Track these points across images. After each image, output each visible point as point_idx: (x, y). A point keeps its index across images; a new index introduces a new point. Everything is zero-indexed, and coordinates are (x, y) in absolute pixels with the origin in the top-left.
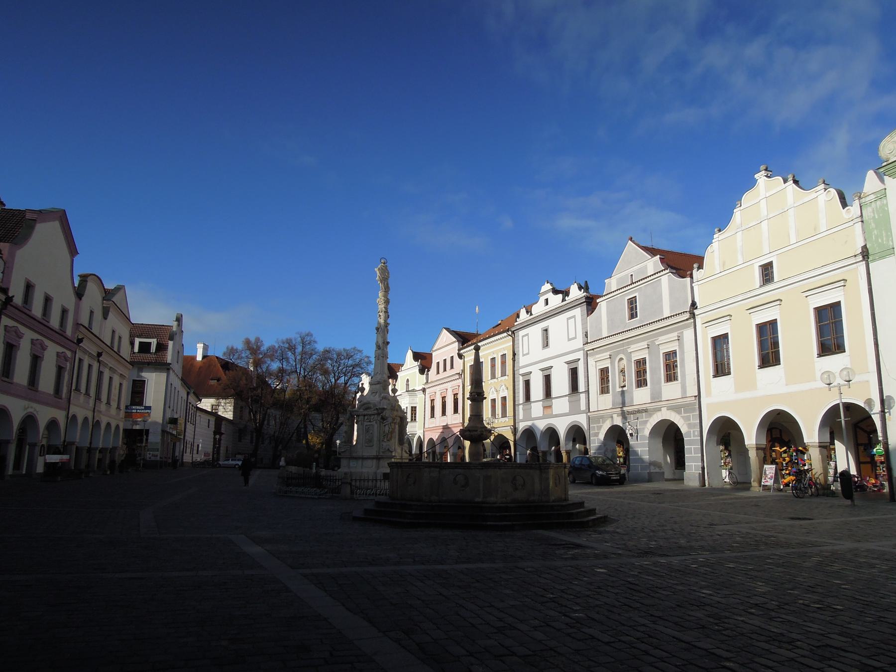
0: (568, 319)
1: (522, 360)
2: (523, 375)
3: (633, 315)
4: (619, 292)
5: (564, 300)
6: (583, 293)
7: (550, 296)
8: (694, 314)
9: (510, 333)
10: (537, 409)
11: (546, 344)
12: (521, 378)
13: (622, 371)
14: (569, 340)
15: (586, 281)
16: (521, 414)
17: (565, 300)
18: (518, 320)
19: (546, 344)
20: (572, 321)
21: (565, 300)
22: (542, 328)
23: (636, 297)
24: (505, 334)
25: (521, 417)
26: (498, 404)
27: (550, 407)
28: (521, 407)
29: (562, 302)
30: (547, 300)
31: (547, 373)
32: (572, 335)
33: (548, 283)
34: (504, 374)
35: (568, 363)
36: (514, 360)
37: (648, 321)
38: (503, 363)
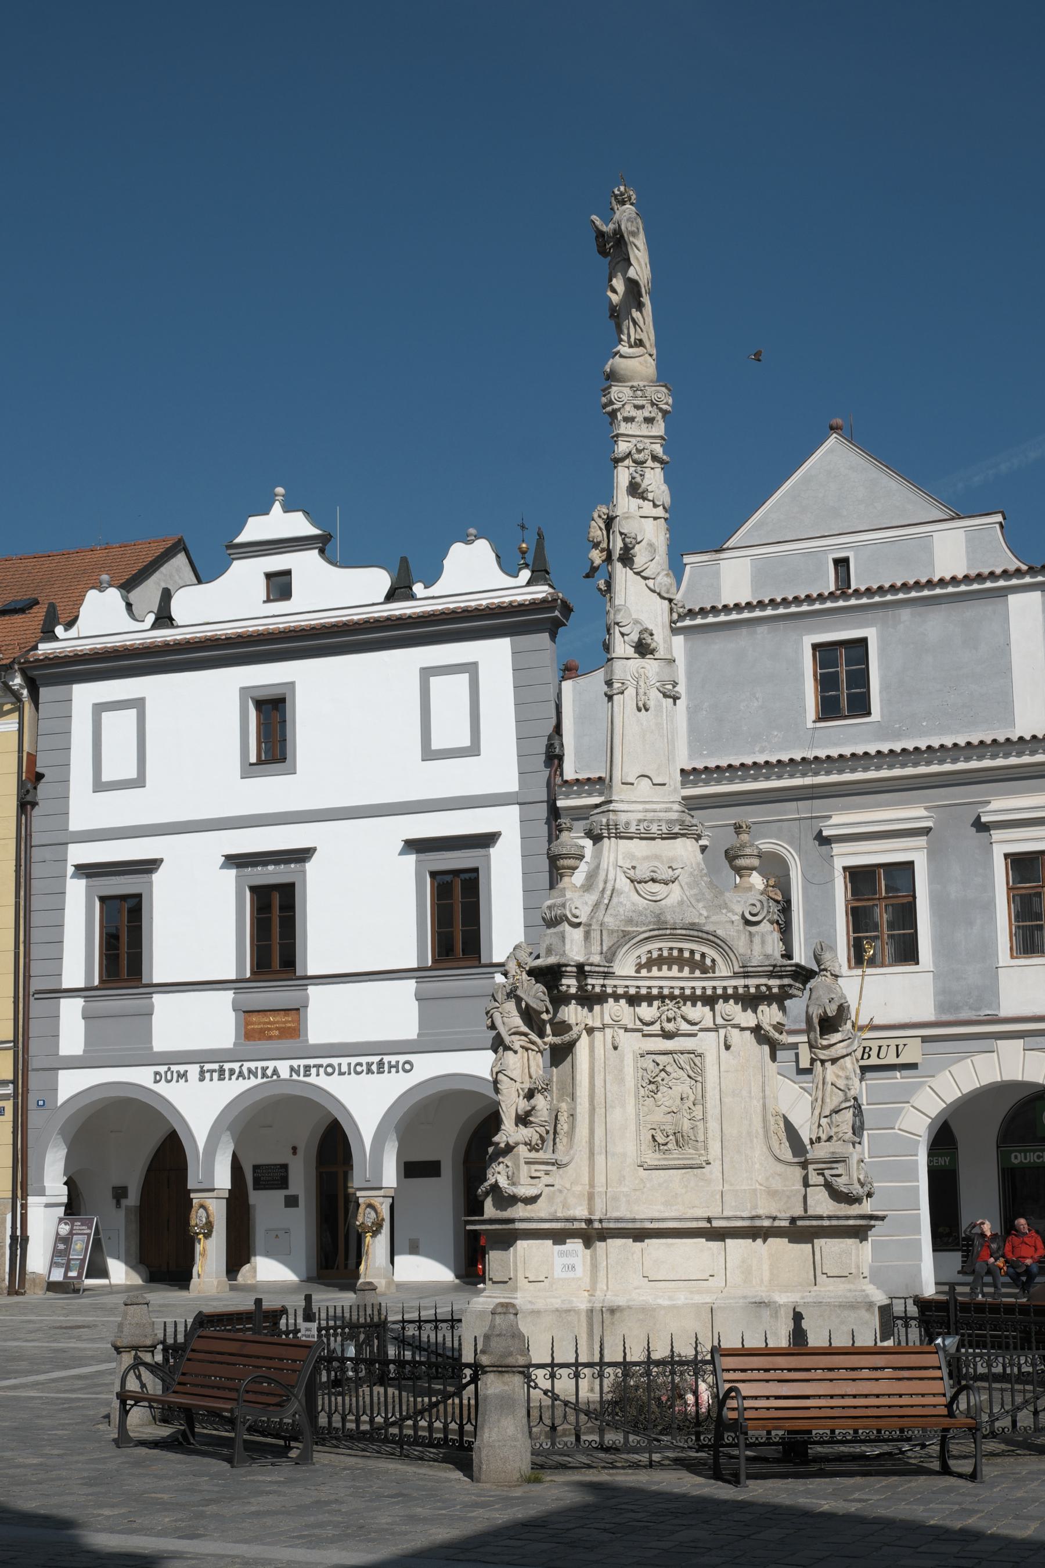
0: (427, 673)
5: (399, 591)
6: (529, 583)
14: (429, 754)
17: (412, 597)
18: (59, 631)
21: (412, 597)
22: (244, 690)
27: (297, 1011)
29: (390, 597)
31: (272, 875)
36: (26, 804)
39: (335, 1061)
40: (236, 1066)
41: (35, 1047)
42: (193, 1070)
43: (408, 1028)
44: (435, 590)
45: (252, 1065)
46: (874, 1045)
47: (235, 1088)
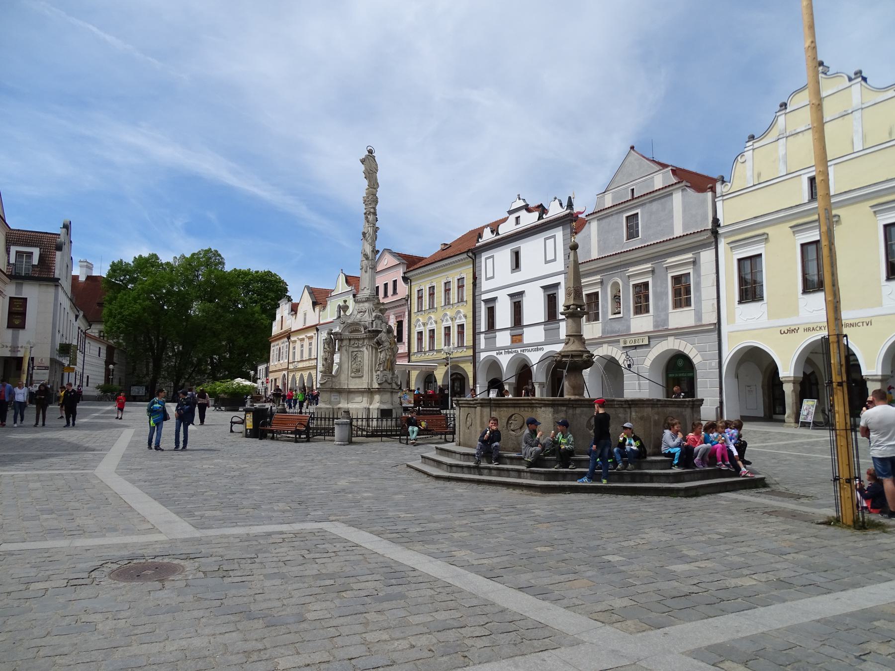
1: (485, 285)
2: (486, 301)
3: (632, 233)
4: (616, 208)
5: (540, 218)
7: (523, 214)
8: (717, 232)
9: (470, 254)
10: (503, 339)
11: (517, 265)
12: (483, 303)
13: (615, 296)
14: (546, 262)
15: (570, 198)
16: (482, 343)
17: (543, 218)
18: (480, 240)
19: (517, 265)
20: (550, 242)
21: (543, 218)
23: (638, 213)
24: (465, 256)
25: (483, 346)
26: (453, 332)
27: (521, 335)
28: (482, 336)
29: (539, 219)
30: (517, 218)
32: (550, 256)
33: (519, 199)
34: (461, 300)
35: (545, 288)
37: (628, 248)
38: (461, 287)
39: (529, 348)
40: (510, 350)
41: (477, 347)
42: (503, 351)
43: (542, 339)
44: (547, 216)
45: (513, 350)
46: (637, 339)
47: (511, 355)
